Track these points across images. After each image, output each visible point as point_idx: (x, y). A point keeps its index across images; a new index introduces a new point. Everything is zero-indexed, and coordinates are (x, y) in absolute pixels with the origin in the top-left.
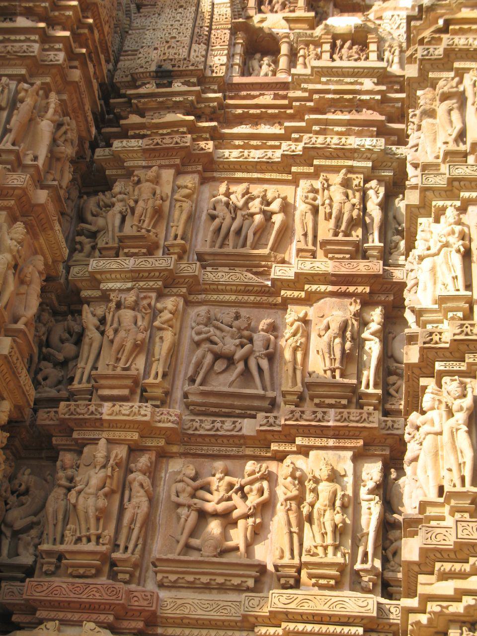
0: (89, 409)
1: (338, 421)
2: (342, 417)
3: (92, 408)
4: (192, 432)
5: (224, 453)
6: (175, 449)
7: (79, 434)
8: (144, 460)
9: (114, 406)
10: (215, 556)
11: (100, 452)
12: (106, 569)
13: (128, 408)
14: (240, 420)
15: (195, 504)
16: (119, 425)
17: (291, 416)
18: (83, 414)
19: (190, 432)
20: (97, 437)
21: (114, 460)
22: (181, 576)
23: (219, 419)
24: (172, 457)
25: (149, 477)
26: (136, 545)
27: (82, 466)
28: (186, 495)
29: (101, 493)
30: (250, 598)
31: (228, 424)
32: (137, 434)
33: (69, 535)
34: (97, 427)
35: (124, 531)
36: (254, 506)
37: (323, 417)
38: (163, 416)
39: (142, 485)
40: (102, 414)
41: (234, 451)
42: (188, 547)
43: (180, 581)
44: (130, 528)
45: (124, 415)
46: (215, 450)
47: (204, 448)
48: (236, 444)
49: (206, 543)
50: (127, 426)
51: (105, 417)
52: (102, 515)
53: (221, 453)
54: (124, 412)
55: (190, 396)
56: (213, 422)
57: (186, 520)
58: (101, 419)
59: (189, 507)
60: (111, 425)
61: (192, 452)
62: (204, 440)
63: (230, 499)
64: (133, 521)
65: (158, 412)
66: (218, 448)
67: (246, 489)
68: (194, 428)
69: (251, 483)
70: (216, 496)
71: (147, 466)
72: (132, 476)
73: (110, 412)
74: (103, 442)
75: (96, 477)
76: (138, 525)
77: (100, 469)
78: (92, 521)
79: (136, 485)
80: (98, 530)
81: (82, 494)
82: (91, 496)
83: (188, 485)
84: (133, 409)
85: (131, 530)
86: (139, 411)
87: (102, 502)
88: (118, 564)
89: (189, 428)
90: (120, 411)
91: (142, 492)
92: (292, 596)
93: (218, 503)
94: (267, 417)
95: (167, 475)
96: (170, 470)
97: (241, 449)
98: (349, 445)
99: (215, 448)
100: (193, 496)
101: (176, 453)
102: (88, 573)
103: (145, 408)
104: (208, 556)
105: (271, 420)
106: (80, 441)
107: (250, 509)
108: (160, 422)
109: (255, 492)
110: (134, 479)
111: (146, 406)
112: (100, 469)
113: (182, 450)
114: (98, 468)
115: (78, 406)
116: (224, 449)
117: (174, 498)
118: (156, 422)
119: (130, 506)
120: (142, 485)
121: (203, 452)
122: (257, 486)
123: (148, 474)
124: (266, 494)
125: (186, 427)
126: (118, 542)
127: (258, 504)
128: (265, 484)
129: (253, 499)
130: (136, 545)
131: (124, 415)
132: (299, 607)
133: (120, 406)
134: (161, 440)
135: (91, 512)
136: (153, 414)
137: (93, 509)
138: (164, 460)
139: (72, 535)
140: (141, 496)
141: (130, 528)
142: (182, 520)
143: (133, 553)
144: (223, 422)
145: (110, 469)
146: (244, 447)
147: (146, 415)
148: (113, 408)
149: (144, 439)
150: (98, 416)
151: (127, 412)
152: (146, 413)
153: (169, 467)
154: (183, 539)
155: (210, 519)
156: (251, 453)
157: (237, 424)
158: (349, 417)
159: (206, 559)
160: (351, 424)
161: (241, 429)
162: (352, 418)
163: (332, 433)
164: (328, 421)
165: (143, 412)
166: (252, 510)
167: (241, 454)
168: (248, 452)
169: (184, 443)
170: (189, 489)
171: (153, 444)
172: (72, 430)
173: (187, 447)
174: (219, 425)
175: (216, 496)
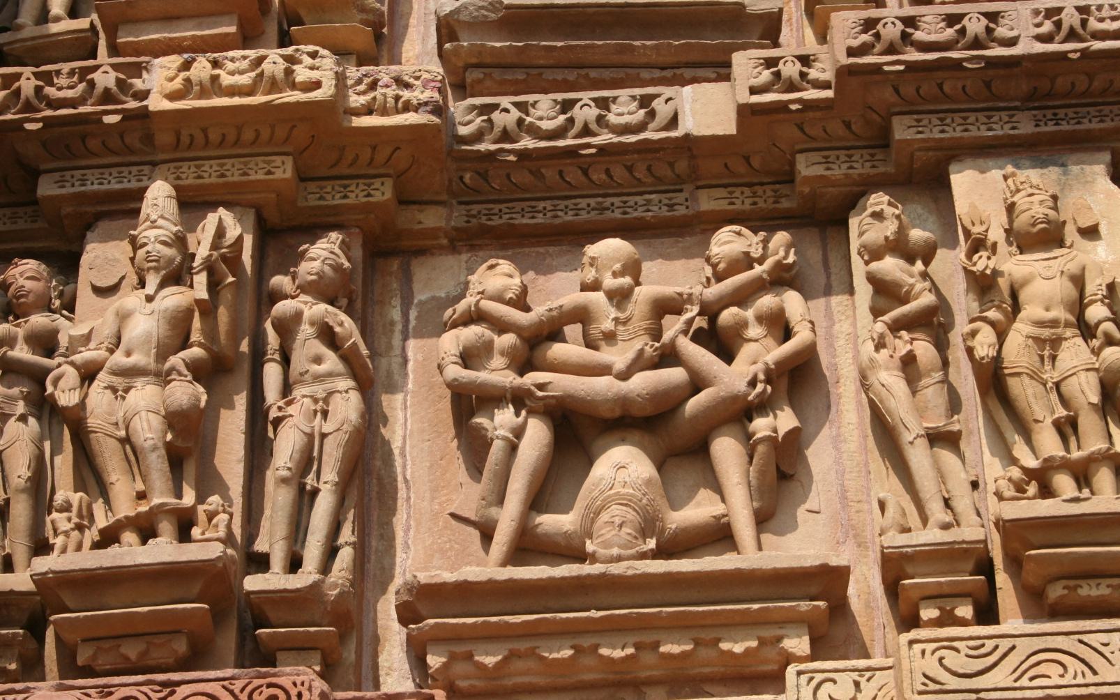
0: (92, 84)
1: (1041, 38)
2: (1058, 25)
3: (105, 79)
4: (493, 147)
5: (618, 214)
6: (432, 218)
7: (61, 183)
8: (323, 253)
9: (187, 66)
10: (643, 556)
11: (154, 225)
12: (228, 641)
13: (244, 64)
14: (668, 91)
15: (541, 387)
16: (214, 136)
17: (865, 38)
18: (72, 103)
19: (483, 147)
20: (134, 185)
21: (215, 246)
22: (523, 646)
23: (586, 96)
24: (421, 252)
25: (349, 311)
26: (331, 551)
27: (85, 297)
28: (498, 361)
29: (176, 360)
30: (819, 677)
31: (625, 109)
32: (289, 161)
33: (64, 526)
34: (132, 151)
35: (278, 501)
36: (768, 372)
37: (989, 31)
38: (379, 92)
39: (328, 335)
40: (144, 95)
41: (653, 207)
42: (527, 546)
43: (519, 665)
44: (302, 487)
45: (233, 91)
46: (584, 211)
47: (541, 205)
48: (660, 180)
49: (604, 517)
50: (248, 135)
51: (157, 103)
52: (188, 444)
53: (608, 214)
54: (226, 80)
55: (461, 35)
56: (567, 106)
57: (513, 448)
58: (144, 114)
59: (519, 399)
60: (185, 139)
61: (496, 221)
62: (537, 174)
63: (668, 357)
64: (308, 460)
65: (359, 81)
66: (592, 202)
67: (728, 315)
68: (497, 130)
69: (741, 298)
70: (618, 356)
71: (337, 268)
72: (283, 307)
73: (177, 84)
74: (159, 196)
75: (145, 315)
76: (330, 475)
77: (162, 285)
78: (157, 464)
79: (307, 344)
80: (179, 495)
81: (103, 378)
82: (139, 382)
83: (501, 326)
84: (266, 66)
85: (305, 498)
86: (289, 72)
87: (185, 392)
88: (272, 615)
89: (478, 137)
90: (215, 79)
91: (332, 361)
92: (990, 644)
93: (624, 376)
94: (770, 63)
95: (413, 314)
96: (421, 296)
97: (680, 198)
98: (1095, 125)
99: (583, 203)
100: (524, 365)
101: (433, 233)
102: (158, 656)
103: (307, 60)
104: (619, 559)
105: (790, 69)
106: (67, 209)
107: (753, 383)
108: (369, 110)
109: (754, 331)
110: (298, 316)
111: (313, 55)
112: (162, 285)
113: (458, 218)
114: (152, 281)
115: (47, 78)
116: (616, 200)
117: (455, 371)
118: (357, 113)
119: (290, 410)
120: (328, 335)
121: (540, 219)
122: (767, 301)
123: (344, 302)
124: (802, 336)
125: (463, 131)
126: (260, 546)
127: (780, 364)
128: (792, 302)
129: (759, 354)
130: (331, 551)
131: (233, 91)
132: (1024, 682)
133: (216, 64)
134: (377, 183)
135: (149, 431)
136: (340, 78)
137: (156, 422)
138: (395, 264)
139: (80, 528)
140: (330, 375)
141: (302, 487)
142: (497, 450)
143: (325, 568)
144: (603, 104)
145: (201, 280)
146: (688, 188)
147: (317, 85)
148: (183, 75)
149: (312, 186)
150: (132, 104)
151: (245, 79)
152: (315, 75)
153: (416, 287)
154: (507, 519)
155: (600, 442)
156: (722, 205)
157: (657, 104)
158: (1084, 23)
159: (616, 569)
160: (1098, 45)
161: (673, 122)
162: (1094, 24)
163: (1025, 87)
164: (1012, 42)
165: (302, 74)
166: (760, 387)
167: (681, 211)
168: (708, 202)
169: (463, 196)
170: (508, 340)
171: (352, 200)
172: (34, 175)
173: (475, 209)
174: (593, 112)
175: (618, 356)
